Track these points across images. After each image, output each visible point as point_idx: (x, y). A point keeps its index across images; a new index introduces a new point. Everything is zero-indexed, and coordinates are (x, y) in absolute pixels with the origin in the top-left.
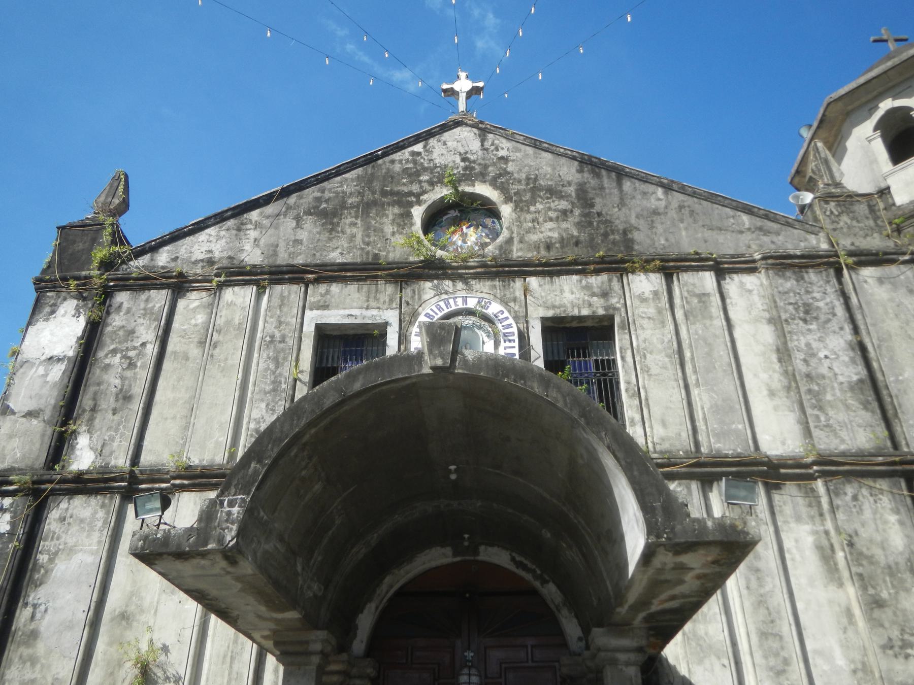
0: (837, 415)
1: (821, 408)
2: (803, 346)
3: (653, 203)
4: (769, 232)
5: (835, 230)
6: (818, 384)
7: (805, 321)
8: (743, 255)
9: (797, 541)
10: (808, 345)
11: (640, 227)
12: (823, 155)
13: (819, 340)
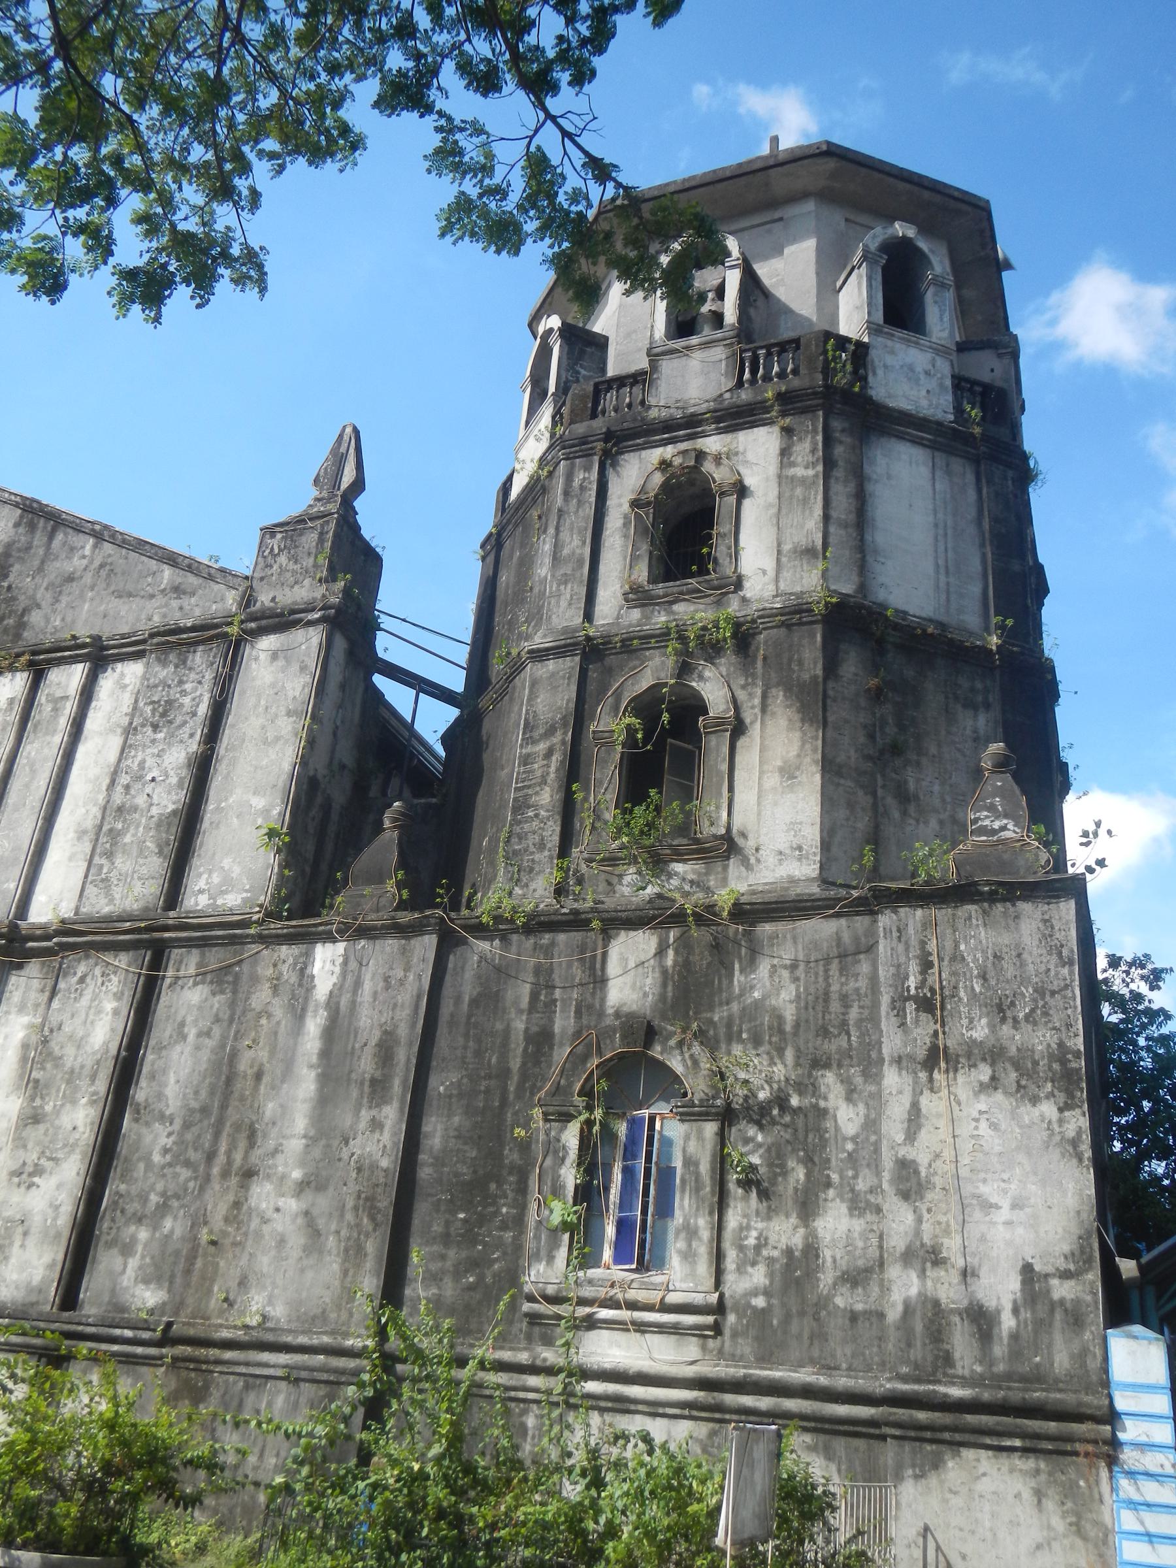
0: (123, 863)
2: (135, 767)
3: (77, 563)
4: (184, 593)
5: (262, 579)
6: (125, 821)
7: (155, 727)
8: (134, 634)
9: (6, 1037)
10: (142, 765)
11: (43, 604)
12: (343, 449)
13: (158, 756)
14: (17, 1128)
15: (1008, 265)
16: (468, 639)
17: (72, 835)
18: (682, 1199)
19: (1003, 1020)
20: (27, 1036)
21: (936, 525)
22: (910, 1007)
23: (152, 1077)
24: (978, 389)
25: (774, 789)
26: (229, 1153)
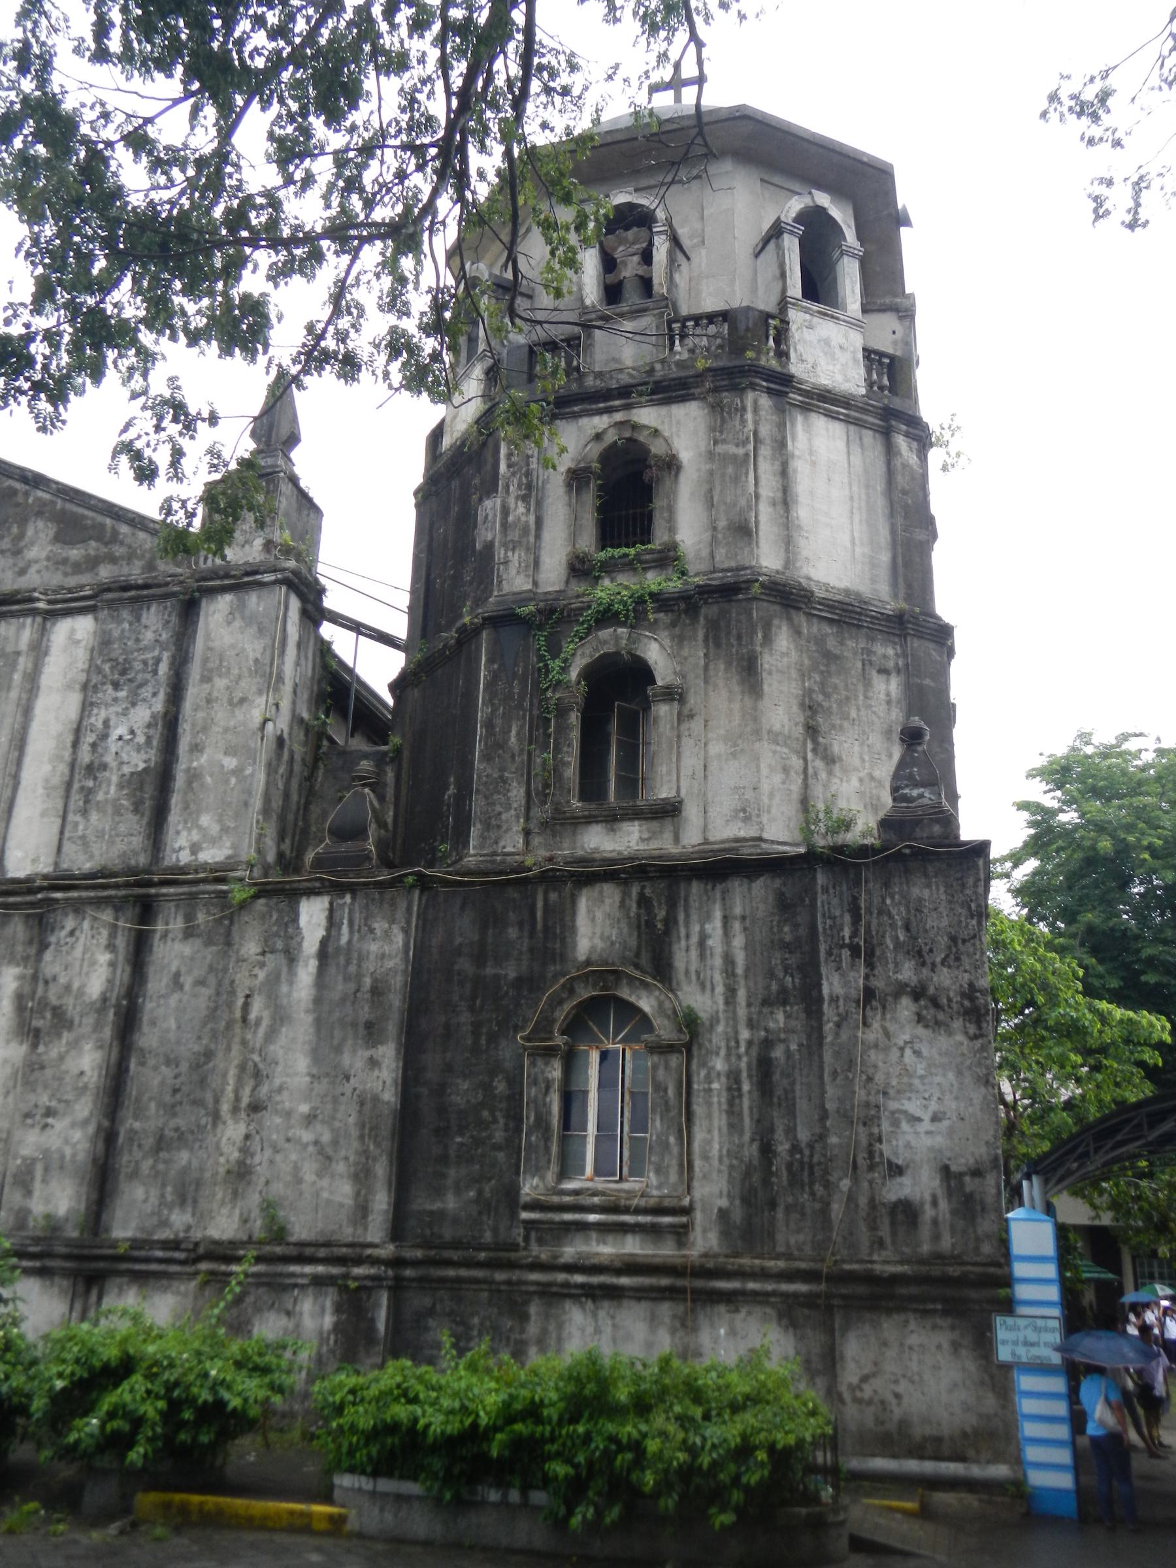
1: (85, 812)
2: (100, 725)
6: (95, 779)
7: (116, 686)
10: (106, 723)
14: (24, 1075)
15: (907, 222)
16: (408, 587)
17: (40, 791)
18: (653, 1121)
19: (924, 964)
20: (21, 986)
21: (852, 498)
22: (846, 953)
23: (153, 1023)
24: (887, 361)
25: (719, 756)
26: (236, 1092)
